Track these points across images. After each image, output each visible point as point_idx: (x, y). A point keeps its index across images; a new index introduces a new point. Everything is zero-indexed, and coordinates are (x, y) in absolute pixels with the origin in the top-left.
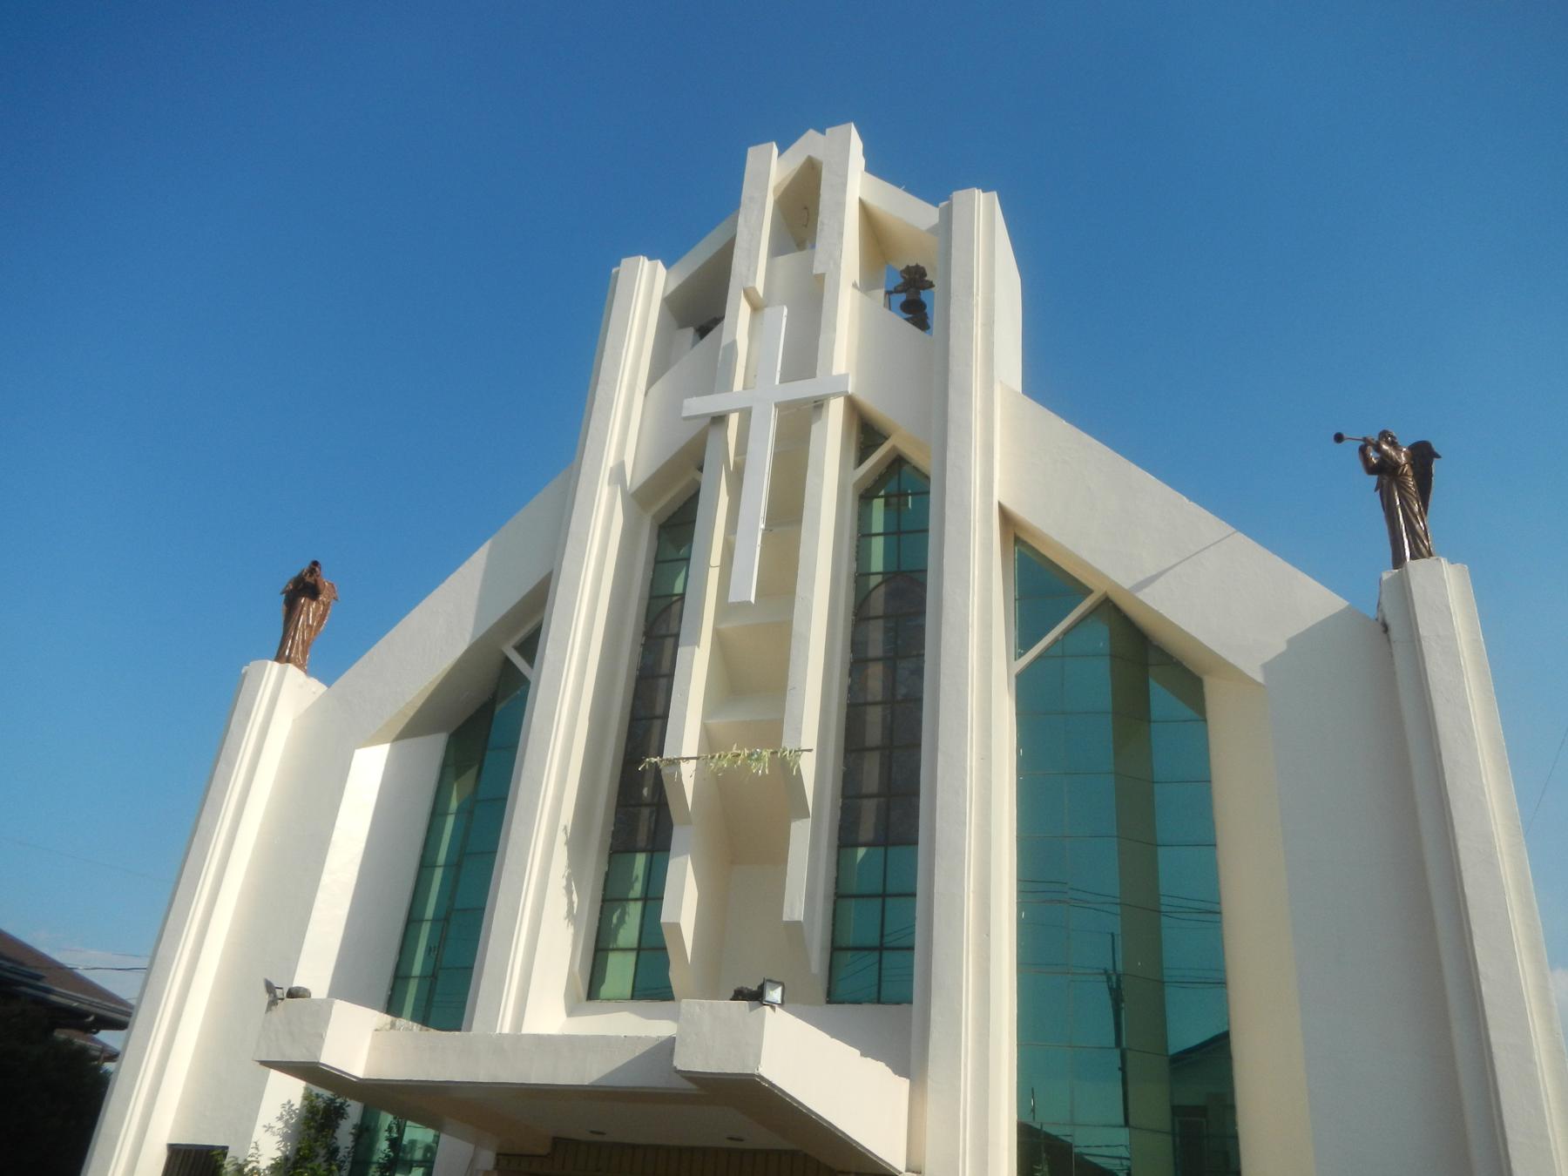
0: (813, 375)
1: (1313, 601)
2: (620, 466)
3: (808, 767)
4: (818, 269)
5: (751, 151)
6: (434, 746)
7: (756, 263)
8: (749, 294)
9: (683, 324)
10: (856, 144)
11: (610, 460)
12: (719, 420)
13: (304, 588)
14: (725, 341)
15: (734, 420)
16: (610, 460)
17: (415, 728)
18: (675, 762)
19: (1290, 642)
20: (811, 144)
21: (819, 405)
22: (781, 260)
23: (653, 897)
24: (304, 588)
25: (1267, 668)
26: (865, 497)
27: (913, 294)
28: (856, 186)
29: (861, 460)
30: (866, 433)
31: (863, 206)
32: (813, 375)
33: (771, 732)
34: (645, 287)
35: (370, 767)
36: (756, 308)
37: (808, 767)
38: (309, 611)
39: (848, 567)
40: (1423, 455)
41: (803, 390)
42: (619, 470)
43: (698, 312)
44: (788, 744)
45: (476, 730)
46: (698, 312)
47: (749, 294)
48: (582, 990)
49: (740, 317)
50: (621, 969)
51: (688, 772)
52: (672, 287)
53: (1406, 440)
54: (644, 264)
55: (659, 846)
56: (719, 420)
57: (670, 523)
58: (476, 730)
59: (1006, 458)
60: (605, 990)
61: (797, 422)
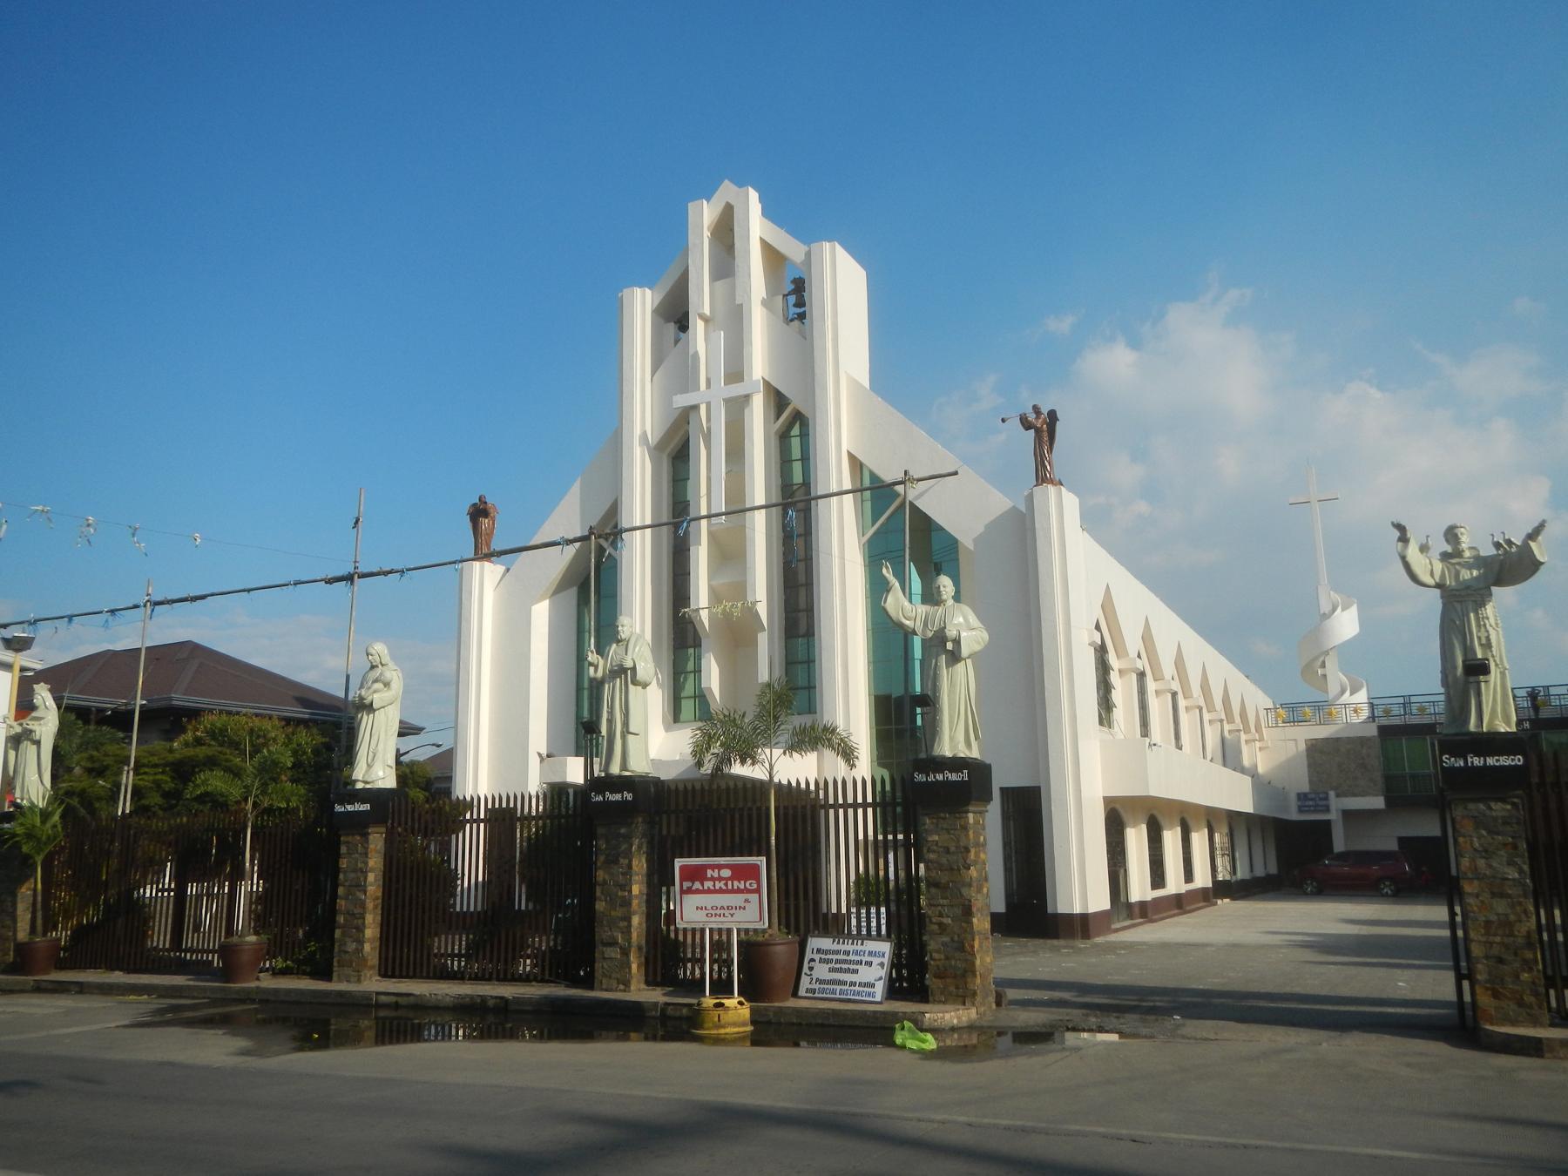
0: (742, 380)
1: (999, 503)
2: (644, 434)
3: (762, 609)
4: (738, 302)
5: (690, 205)
6: (572, 594)
7: (703, 297)
8: (702, 317)
9: (668, 320)
10: (753, 195)
11: (638, 432)
12: (696, 408)
13: (479, 512)
14: (691, 352)
15: (703, 408)
16: (638, 432)
17: (562, 587)
18: (697, 610)
19: (987, 527)
20: (727, 191)
21: (747, 398)
22: (719, 284)
23: (698, 671)
24: (479, 512)
25: (975, 541)
26: (784, 436)
27: (796, 297)
28: (756, 227)
29: (778, 416)
30: (778, 401)
31: (764, 243)
32: (742, 380)
33: (740, 589)
34: (642, 304)
35: (541, 612)
36: (706, 320)
37: (762, 609)
38: (485, 522)
39: (776, 482)
40: (1053, 416)
41: (737, 390)
42: (644, 434)
43: (675, 314)
44: (750, 599)
45: (591, 587)
46: (675, 314)
47: (702, 317)
48: (671, 718)
49: (698, 327)
50: (688, 707)
51: (704, 615)
52: (656, 303)
53: (1045, 411)
54: (638, 291)
55: (697, 644)
56: (696, 408)
57: (676, 455)
58: (591, 587)
59: (846, 432)
60: (683, 716)
61: (736, 407)
